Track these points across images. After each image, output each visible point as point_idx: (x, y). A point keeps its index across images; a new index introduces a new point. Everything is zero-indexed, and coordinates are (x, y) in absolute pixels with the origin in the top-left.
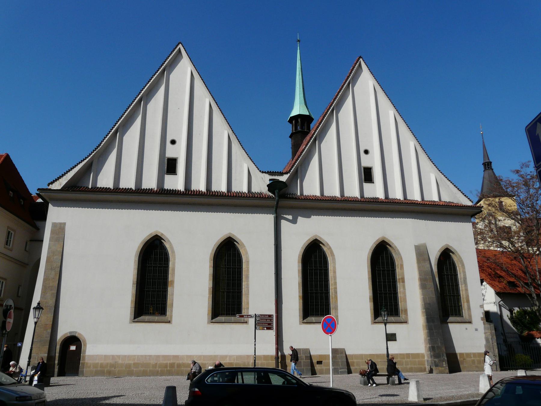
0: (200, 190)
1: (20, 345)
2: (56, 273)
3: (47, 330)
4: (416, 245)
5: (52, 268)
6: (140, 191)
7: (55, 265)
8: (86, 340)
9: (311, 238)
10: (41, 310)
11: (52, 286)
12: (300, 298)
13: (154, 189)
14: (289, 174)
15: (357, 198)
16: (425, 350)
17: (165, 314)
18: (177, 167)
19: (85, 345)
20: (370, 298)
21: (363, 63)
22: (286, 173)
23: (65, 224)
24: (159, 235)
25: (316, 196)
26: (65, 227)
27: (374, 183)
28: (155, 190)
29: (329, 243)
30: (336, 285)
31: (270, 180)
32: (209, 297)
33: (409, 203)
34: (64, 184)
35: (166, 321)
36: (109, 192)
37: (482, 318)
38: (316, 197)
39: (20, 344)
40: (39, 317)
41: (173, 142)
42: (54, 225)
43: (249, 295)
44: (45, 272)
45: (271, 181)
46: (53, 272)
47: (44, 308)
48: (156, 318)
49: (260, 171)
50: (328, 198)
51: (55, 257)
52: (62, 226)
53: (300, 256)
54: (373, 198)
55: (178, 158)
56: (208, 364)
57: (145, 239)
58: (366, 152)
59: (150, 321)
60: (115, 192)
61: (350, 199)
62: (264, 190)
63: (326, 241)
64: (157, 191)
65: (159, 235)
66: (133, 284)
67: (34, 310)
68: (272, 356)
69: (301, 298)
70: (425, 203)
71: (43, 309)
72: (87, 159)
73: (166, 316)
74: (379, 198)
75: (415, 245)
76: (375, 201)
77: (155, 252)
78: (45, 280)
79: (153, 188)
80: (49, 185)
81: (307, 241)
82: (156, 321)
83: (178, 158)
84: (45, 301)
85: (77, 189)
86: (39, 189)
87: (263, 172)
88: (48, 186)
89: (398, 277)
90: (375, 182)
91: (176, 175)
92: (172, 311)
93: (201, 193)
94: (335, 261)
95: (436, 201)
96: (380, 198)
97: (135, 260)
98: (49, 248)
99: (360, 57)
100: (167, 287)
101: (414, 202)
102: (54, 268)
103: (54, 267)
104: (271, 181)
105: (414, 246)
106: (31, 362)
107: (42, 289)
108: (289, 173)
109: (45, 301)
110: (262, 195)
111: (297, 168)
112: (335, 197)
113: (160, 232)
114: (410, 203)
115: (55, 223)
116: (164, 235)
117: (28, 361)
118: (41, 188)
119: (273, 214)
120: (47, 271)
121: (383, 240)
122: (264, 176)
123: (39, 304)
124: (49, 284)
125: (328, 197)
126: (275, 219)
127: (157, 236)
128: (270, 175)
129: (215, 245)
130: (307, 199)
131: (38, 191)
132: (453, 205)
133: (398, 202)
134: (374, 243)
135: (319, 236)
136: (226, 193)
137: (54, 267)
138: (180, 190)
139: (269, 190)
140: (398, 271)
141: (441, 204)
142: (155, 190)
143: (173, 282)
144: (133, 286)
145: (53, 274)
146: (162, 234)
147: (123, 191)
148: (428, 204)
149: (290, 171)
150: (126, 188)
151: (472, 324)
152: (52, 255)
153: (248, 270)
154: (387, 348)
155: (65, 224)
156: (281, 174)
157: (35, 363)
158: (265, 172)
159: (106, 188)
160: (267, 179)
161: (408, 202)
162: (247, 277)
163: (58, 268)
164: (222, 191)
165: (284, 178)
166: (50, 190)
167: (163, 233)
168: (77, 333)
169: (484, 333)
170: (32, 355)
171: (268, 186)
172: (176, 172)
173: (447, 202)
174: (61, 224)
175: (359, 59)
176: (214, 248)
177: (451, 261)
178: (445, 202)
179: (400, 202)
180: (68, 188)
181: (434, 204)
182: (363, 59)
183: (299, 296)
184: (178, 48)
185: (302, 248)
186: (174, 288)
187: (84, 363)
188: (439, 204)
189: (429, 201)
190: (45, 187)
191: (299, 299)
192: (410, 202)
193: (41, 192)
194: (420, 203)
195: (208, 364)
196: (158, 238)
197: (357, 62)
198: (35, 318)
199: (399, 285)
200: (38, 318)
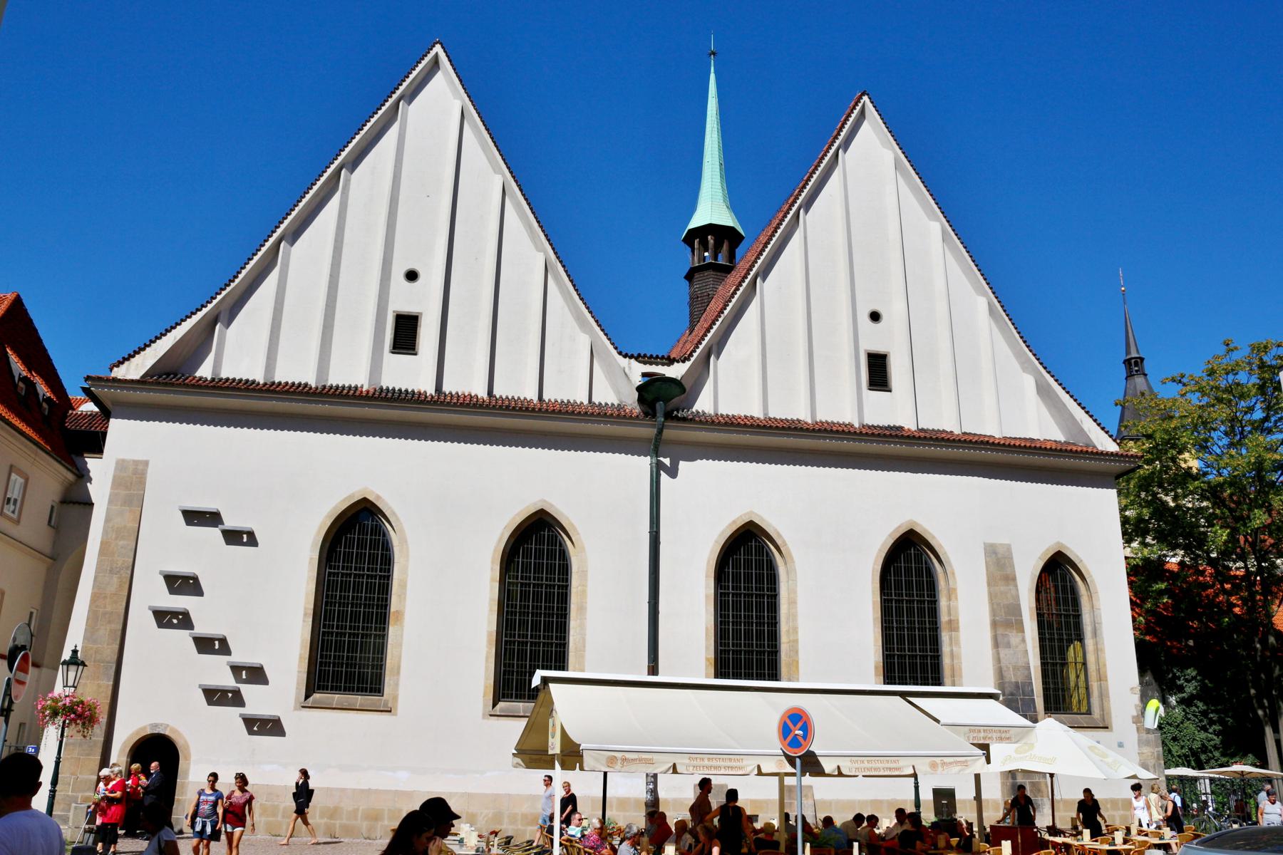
0: (473, 395)
1: (33, 750)
4: (987, 542)
6: (329, 390)
7: (120, 563)
8: (188, 746)
9: (738, 518)
10: (81, 668)
12: (708, 663)
13: (362, 387)
14: (688, 364)
15: (852, 426)
16: (1003, 792)
17: (379, 692)
18: (419, 335)
19: (188, 758)
20: (876, 668)
21: (869, 106)
22: (683, 362)
24: (371, 498)
25: (752, 418)
27: (890, 391)
28: (364, 390)
29: (781, 533)
30: (797, 633)
31: (644, 375)
32: (488, 653)
33: (974, 440)
34: (149, 367)
35: (382, 709)
36: (254, 390)
37: (1133, 717)
38: (752, 419)
39: (32, 748)
40: (76, 685)
41: (412, 276)
42: (121, 465)
43: (584, 651)
44: (96, 578)
45: (647, 379)
46: (115, 580)
47: (86, 664)
48: (358, 699)
49: (620, 353)
50: (781, 423)
51: (121, 543)
53: (711, 562)
54: (889, 428)
55: (421, 314)
56: (483, 816)
57: (335, 508)
58: (875, 317)
59: (344, 707)
60: (268, 391)
61: (834, 429)
62: (630, 400)
63: (774, 527)
64: (368, 392)
65: (371, 499)
66: (305, 615)
67: (65, 667)
68: (637, 801)
69: (711, 663)
70: (1012, 444)
71: (86, 666)
72: (205, 311)
73: (383, 696)
74: (902, 428)
75: (984, 543)
76: (893, 434)
78: (95, 598)
79: (359, 386)
80: (111, 370)
81: (730, 525)
82: (358, 708)
83: (421, 314)
84: (95, 646)
85: (178, 380)
86: (88, 378)
87: (625, 356)
88: (111, 371)
89: (944, 617)
90: (893, 390)
91: (416, 354)
92: (397, 685)
93: (475, 400)
94: (796, 576)
95: (1035, 438)
96: (906, 427)
97: (311, 559)
98: (107, 520)
99: (863, 94)
100: (386, 626)
101: (986, 439)
102: (118, 570)
104: (647, 379)
105: (983, 546)
106: (57, 793)
107: (88, 619)
108: (689, 360)
109: (95, 646)
110: (625, 411)
111: (707, 350)
112: (799, 421)
113: (373, 492)
114: (976, 441)
115: (123, 461)
116: (383, 500)
117: (50, 791)
118: (93, 374)
119: (646, 456)
120: (101, 574)
121: (909, 529)
122: (629, 364)
123: (75, 652)
124: (105, 607)
125: (782, 420)
126: (654, 470)
127: (365, 500)
128: (645, 363)
130: (732, 423)
131: (86, 381)
132: (1074, 448)
133: (948, 439)
134: (890, 535)
135: (758, 515)
136: (535, 402)
137: (117, 568)
138: (425, 392)
139: (641, 400)
140: (943, 603)
141: (1048, 447)
142: (364, 390)
143: (400, 614)
144: (304, 621)
145: (114, 584)
146: (378, 497)
147: (288, 389)
148: (1017, 444)
149: (691, 355)
150: (293, 384)
151: (1112, 731)
152: (114, 536)
153: (583, 593)
154: (915, 787)
155: (146, 463)
156: (670, 361)
157: (68, 796)
158: (631, 357)
159: (247, 381)
160: (637, 371)
161: (971, 438)
162: (582, 609)
163: (127, 568)
164: (525, 399)
165: (676, 371)
166: (115, 380)
167: (380, 494)
168: (168, 729)
169: (1139, 753)
170: (59, 776)
171: (639, 389)
172: (416, 347)
173: (1060, 442)
175: (860, 98)
176: (502, 534)
177: (1068, 584)
178: (1055, 441)
179: (954, 439)
180: (160, 377)
181: (1033, 445)
182: (870, 98)
183: (707, 659)
184: (432, 53)
185: (716, 542)
186: (403, 630)
187: (185, 800)
188: (1043, 447)
189: (1020, 438)
190: (103, 373)
191: (707, 667)
192: (976, 438)
193: (93, 386)
194: (999, 443)
195: (483, 816)
196: (368, 506)
197: (856, 104)
198: (67, 686)
199: (945, 637)
200: (73, 686)
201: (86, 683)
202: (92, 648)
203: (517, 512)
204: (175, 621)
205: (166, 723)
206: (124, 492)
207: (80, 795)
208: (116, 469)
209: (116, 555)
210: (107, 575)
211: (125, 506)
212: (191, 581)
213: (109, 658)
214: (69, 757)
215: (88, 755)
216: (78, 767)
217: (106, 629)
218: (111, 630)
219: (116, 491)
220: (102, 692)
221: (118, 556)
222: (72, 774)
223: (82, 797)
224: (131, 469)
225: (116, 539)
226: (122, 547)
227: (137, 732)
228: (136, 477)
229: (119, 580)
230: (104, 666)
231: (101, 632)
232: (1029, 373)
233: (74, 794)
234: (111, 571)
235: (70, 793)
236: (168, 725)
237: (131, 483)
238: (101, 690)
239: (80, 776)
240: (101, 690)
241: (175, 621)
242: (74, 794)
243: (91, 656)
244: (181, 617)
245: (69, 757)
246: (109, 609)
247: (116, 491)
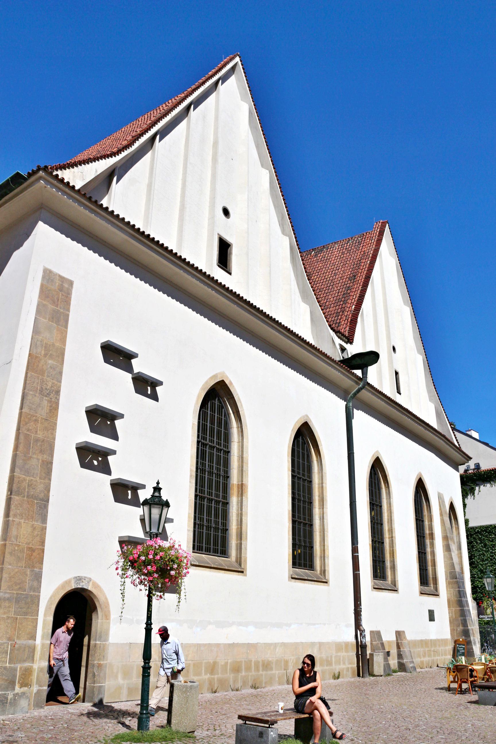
2: (51, 406)
3: (33, 567)
5: (42, 388)
7: (50, 384)
11: (43, 441)
23: (71, 283)
26: (71, 291)
51: (50, 362)
52: (66, 285)
77: (203, 410)
103: (48, 387)
109: (28, 478)
120: (31, 393)
129: (292, 431)
137: (46, 389)
152: (43, 352)
157: (5, 668)
168: (91, 583)
174: (62, 279)
201: (20, 522)
202: (25, 480)
203: (296, 420)
204: (95, 463)
205: (88, 576)
206: (51, 307)
207: (19, 666)
208: (44, 277)
209: (46, 374)
210: (37, 395)
211: (52, 322)
212: (109, 423)
213: (42, 494)
214: (5, 616)
215: (26, 614)
216: (15, 630)
217: (38, 459)
218: (43, 461)
219: (44, 302)
220: (37, 535)
221: (48, 376)
222: (9, 639)
223: (21, 668)
224: (57, 284)
225: (45, 355)
226: (51, 367)
227: (63, 586)
228: (62, 295)
229: (49, 405)
230: (37, 503)
231: (34, 462)
232: (433, 402)
233: (12, 665)
234: (41, 391)
235: (8, 665)
236: (90, 579)
237: (58, 300)
238: (36, 533)
239: (18, 642)
240: (36, 533)
241: (95, 463)
242: (12, 665)
243: (24, 489)
244: (100, 459)
245: (5, 616)
246: (40, 435)
247: (44, 302)
